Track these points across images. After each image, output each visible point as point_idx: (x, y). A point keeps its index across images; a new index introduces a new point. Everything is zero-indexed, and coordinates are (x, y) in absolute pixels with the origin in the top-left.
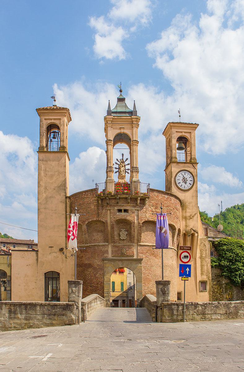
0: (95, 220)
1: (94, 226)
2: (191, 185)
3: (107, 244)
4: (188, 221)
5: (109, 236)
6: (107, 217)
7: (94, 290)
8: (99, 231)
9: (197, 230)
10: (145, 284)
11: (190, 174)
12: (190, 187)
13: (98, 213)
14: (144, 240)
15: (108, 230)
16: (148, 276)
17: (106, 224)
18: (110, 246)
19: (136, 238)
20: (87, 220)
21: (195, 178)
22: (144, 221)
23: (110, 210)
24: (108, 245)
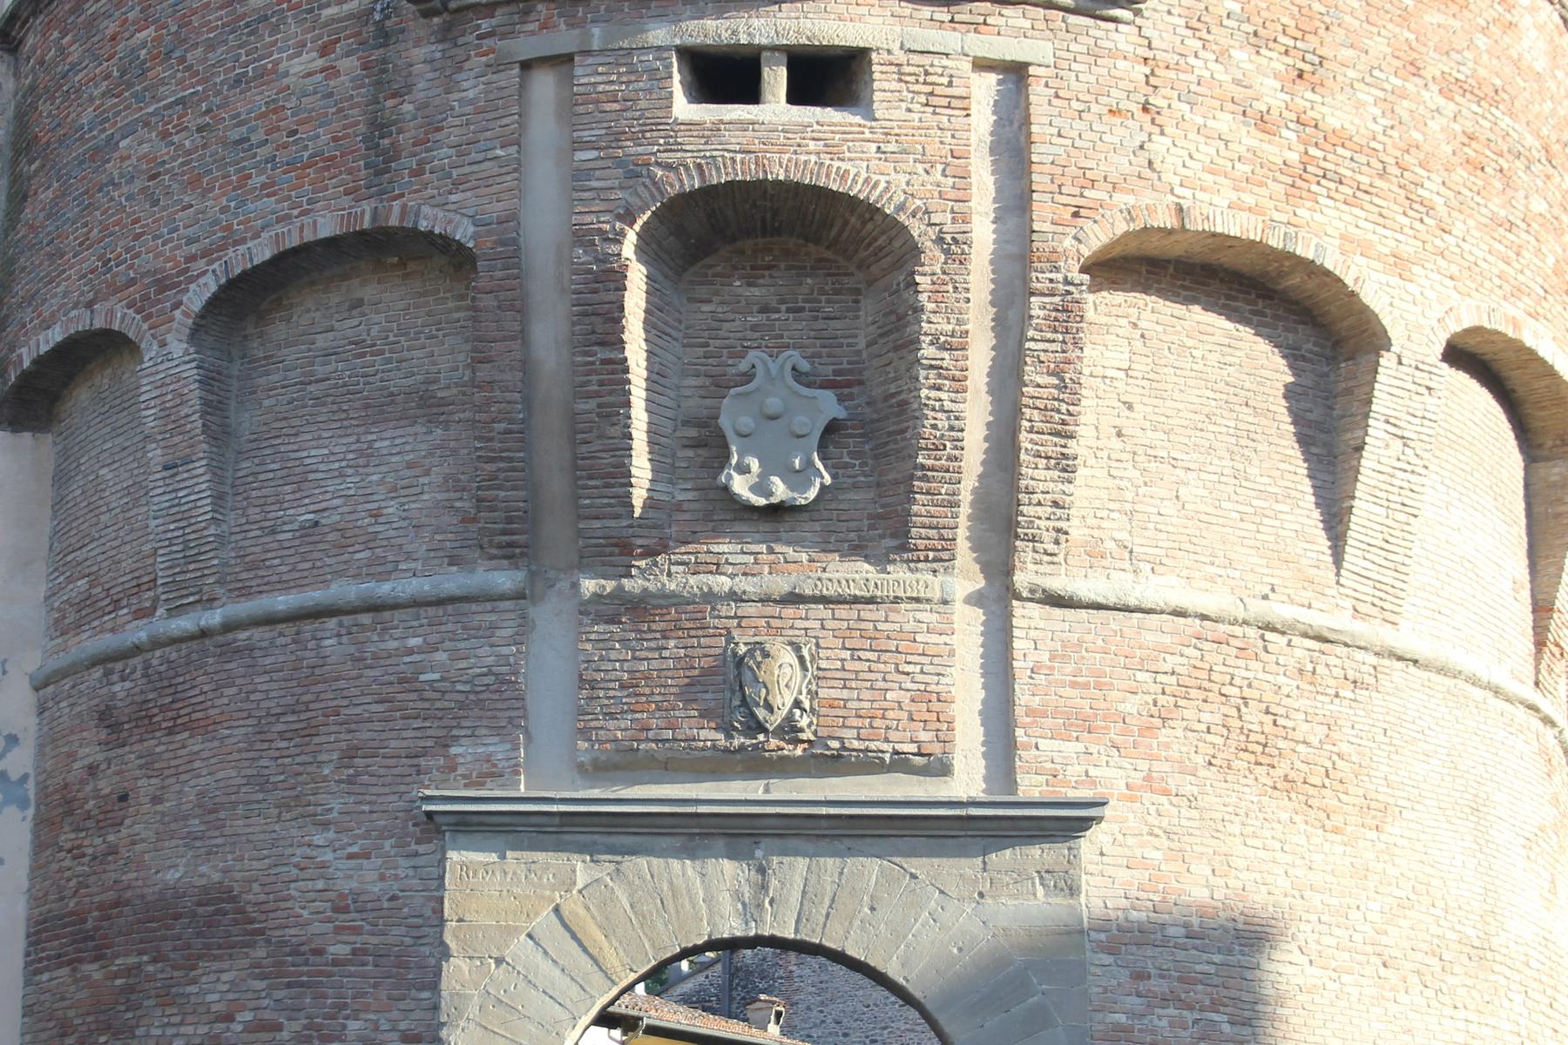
0: (327, 226)
1: (321, 341)
3: (505, 579)
5: (551, 455)
6: (518, 166)
8: (379, 410)
14: (1117, 528)
15: (526, 366)
17: (486, 274)
18: (551, 621)
20: (206, 253)
22: (1121, 228)
23: (564, 60)
24: (520, 596)
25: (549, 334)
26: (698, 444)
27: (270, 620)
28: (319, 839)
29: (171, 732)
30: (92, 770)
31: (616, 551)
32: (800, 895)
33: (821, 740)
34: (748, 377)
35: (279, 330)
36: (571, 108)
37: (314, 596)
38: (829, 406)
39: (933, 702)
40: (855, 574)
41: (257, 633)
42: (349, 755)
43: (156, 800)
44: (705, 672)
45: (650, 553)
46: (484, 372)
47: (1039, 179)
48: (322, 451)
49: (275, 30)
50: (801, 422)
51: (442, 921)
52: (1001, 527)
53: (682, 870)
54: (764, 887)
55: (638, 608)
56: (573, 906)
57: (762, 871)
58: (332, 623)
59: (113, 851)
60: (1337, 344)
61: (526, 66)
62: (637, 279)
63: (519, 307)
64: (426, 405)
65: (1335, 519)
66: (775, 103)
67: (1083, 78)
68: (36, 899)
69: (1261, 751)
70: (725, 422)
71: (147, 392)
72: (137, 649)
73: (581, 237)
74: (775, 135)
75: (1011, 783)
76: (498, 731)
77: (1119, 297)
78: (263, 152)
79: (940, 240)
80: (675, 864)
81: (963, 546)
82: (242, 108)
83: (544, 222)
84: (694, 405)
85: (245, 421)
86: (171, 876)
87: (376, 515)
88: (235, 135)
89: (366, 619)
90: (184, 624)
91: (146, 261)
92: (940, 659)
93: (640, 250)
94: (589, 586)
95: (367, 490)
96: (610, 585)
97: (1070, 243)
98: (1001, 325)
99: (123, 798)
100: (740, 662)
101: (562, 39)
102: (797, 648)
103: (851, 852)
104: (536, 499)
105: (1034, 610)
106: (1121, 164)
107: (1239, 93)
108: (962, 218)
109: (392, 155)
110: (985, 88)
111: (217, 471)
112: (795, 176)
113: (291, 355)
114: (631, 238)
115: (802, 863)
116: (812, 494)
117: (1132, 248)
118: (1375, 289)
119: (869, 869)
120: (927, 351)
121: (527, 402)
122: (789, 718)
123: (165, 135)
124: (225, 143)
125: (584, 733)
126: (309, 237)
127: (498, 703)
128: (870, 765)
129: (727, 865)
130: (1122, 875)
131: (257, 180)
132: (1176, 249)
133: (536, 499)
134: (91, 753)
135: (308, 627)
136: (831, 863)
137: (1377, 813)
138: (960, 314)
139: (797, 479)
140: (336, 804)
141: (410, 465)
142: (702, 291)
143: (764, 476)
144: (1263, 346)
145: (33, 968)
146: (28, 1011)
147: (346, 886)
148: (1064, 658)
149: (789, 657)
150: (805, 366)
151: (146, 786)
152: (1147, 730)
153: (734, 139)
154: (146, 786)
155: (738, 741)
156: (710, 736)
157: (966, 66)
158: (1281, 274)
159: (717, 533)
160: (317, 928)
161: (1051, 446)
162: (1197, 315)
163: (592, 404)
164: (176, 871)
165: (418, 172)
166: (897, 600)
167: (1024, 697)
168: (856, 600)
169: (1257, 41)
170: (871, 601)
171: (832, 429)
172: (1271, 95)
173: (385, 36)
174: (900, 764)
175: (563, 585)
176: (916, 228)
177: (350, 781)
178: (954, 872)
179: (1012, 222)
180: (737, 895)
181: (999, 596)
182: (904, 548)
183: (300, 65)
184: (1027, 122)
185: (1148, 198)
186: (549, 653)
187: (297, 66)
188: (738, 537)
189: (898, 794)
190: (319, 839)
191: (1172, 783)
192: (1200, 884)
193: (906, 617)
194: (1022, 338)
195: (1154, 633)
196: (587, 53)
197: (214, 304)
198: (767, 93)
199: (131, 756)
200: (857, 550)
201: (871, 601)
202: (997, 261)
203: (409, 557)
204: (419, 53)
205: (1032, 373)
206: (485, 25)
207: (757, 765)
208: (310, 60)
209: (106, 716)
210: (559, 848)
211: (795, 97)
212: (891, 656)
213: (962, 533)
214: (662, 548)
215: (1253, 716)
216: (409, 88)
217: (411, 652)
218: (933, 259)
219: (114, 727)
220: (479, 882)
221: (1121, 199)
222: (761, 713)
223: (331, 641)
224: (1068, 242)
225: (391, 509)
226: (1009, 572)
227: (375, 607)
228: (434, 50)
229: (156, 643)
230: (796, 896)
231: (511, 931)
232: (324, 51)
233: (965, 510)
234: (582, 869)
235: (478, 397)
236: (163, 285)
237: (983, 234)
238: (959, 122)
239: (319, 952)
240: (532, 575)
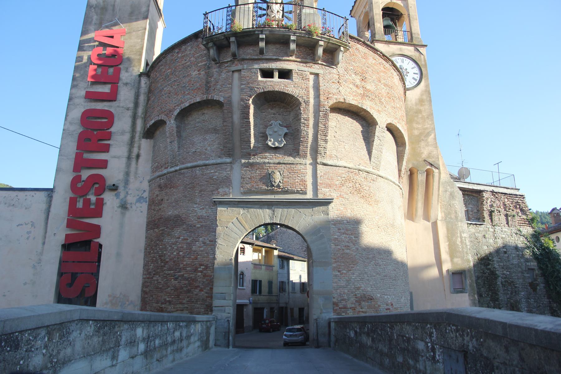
0: (198, 100)
1: (197, 120)
2: (416, 80)
3: (228, 160)
5: (237, 139)
6: (231, 88)
7: (185, 289)
10: (339, 271)
11: (412, 63)
12: (415, 84)
14: (334, 153)
15: (232, 123)
16: (348, 247)
18: (236, 167)
20: (178, 105)
21: (423, 69)
22: (335, 101)
23: (239, 71)
24: (231, 163)
25: (236, 117)
26: (262, 137)
27: (187, 168)
28: (195, 206)
29: (170, 188)
30: (157, 195)
31: (248, 155)
32: (280, 215)
33: (284, 188)
34: (271, 125)
35: (190, 119)
36: (240, 79)
37: (195, 164)
38: (285, 130)
39: (304, 182)
40: (290, 159)
41: (185, 170)
42: (201, 191)
43: (167, 200)
44: (264, 176)
45: (254, 155)
46: (225, 124)
47: (321, 92)
48: (197, 139)
49: (190, 68)
50: (280, 133)
51: (217, 220)
52: (315, 151)
53: (260, 211)
54: (274, 214)
55: (252, 165)
56: (240, 218)
57: (274, 211)
58: (198, 168)
59: (160, 209)
60: (369, 124)
61: (233, 72)
62: (252, 107)
63: (231, 112)
65: (370, 153)
66: (276, 78)
67: (328, 77)
68: (148, 218)
69: (359, 191)
70: (267, 133)
71: (167, 129)
72: (165, 174)
73: (242, 100)
74: (276, 84)
75: (317, 196)
76: (227, 187)
77: (334, 114)
78: (188, 88)
79: (304, 102)
80: (258, 210)
81: (308, 155)
82: (184, 81)
83: (236, 97)
84: (262, 130)
85: (184, 134)
86: (170, 213)
87: (206, 149)
88: (183, 85)
89: (204, 167)
90: (173, 169)
91: (168, 107)
92: (305, 174)
93: (253, 102)
94: (243, 161)
95: (204, 144)
96: (247, 161)
97: (327, 104)
98: (315, 116)
99: (162, 200)
100: (270, 174)
101: (239, 67)
102: (280, 172)
103: (289, 208)
104: (234, 146)
105: (321, 166)
106: (335, 91)
107: (353, 81)
108: (308, 98)
109: (210, 87)
110: (312, 77)
111: (179, 143)
112: (279, 90)
113: (192, 123)
114: (251, 100)
115: (281, 210)
116: (282, 145)
117: (336, 106)
118: (375, 115)
119: (292, 211)
120: (302, 121)
121: (232, 129)
122: (278, 184)
123: (172, 86)
124: (181, 87)
125: (242, 187)
126: (195, 101)
127: (227, 182)
128: (293, 192)
129: (267, 210)
130: (336, 212)
131: (187, 93)
132: (343, 106)
133: (234, 146)
134: (157, 193)
135: (194, 169)
136: (286, 210)
137: (377, 202)
138: (308, 114)
139: (280, 142)
140: (198, 200)
141: (212, 141)
142: (264, 111)
143: (274, 142)
144: (357, 124)
145: (147, 230)
146: (146, 238)
147: (200, 214)
148: (326, 174)
149: (278, 173)
150: (281, 123)
151: (166, 198)
152: (340, 187)
153: (269, 84)
154: (166, 198)
155: (269, 188)
156: (264, 187)
157: (309, 73)
158: (360, 112)
159: (266, 152)
160: (195, 222)
161: (324, 138)
162: (347, 118)
163: (244, 129)
164: (171, 212)
165: (214, 90)
166: (297, 164)
167: (319, 181)
168: (290, 164)
169: (356, 74)
170: (293, 164)
171: (286, 134)
172: (358, 82)
173: (209, 68)
174: (298, 192)
175: (239, 161)
176: (300, 99)
177: (201, 196)
178: (308, 211)
179: (317, 99)
180: (269, 216)
181: (315, 164)
182: (298, 155)
183: (194, 73)
184: (319, 83)
185: (339, 97)
186: (236, 173)
187: (194, 74)
188: (269, 153)
189: (297, 198)
190: (195, 206)
191: (344, 196)
192: (349, 213)
193: (299, 167)
194: (319, 119)
195: (341, 170)
196: (243, 69)
197: (179, 114)
198: (275, 77)
199: (163, 192)
200: (290, 155)
201: (293, 164)
202: (314, 106)
203: (212, 157)
204: (215, 70)
205: (320, 125)
206: (226, 65)
207: (273, 192)
208: (196, 72)
209: (160, 186)
210: (237, 207)
211: (279, 78)
212: (296, 174)
213: (308, 152)
214: (257, 155)
215: (357, 185)
216: (213, 76)
217: (212, 173)
218: (303, 105)
219: (161, 188)
220: (223, 213)
221: (335, 97)
222: (273, 183)
223: (198, 171)
224: (326, 103)
225: (209, 148)
226: (316, 159)
227: (206, 165)
228: (217, 70)
229: (168, 173)
230: (280, 215)
231: (229, 222)
232: (199, 71)
233: (309, 148)
234: (242, 211)
235: (224, 128)
236: (170, 111)
237: (312, 101)
238: (308, 82)
239: (195, 226)
240: (233, 159)
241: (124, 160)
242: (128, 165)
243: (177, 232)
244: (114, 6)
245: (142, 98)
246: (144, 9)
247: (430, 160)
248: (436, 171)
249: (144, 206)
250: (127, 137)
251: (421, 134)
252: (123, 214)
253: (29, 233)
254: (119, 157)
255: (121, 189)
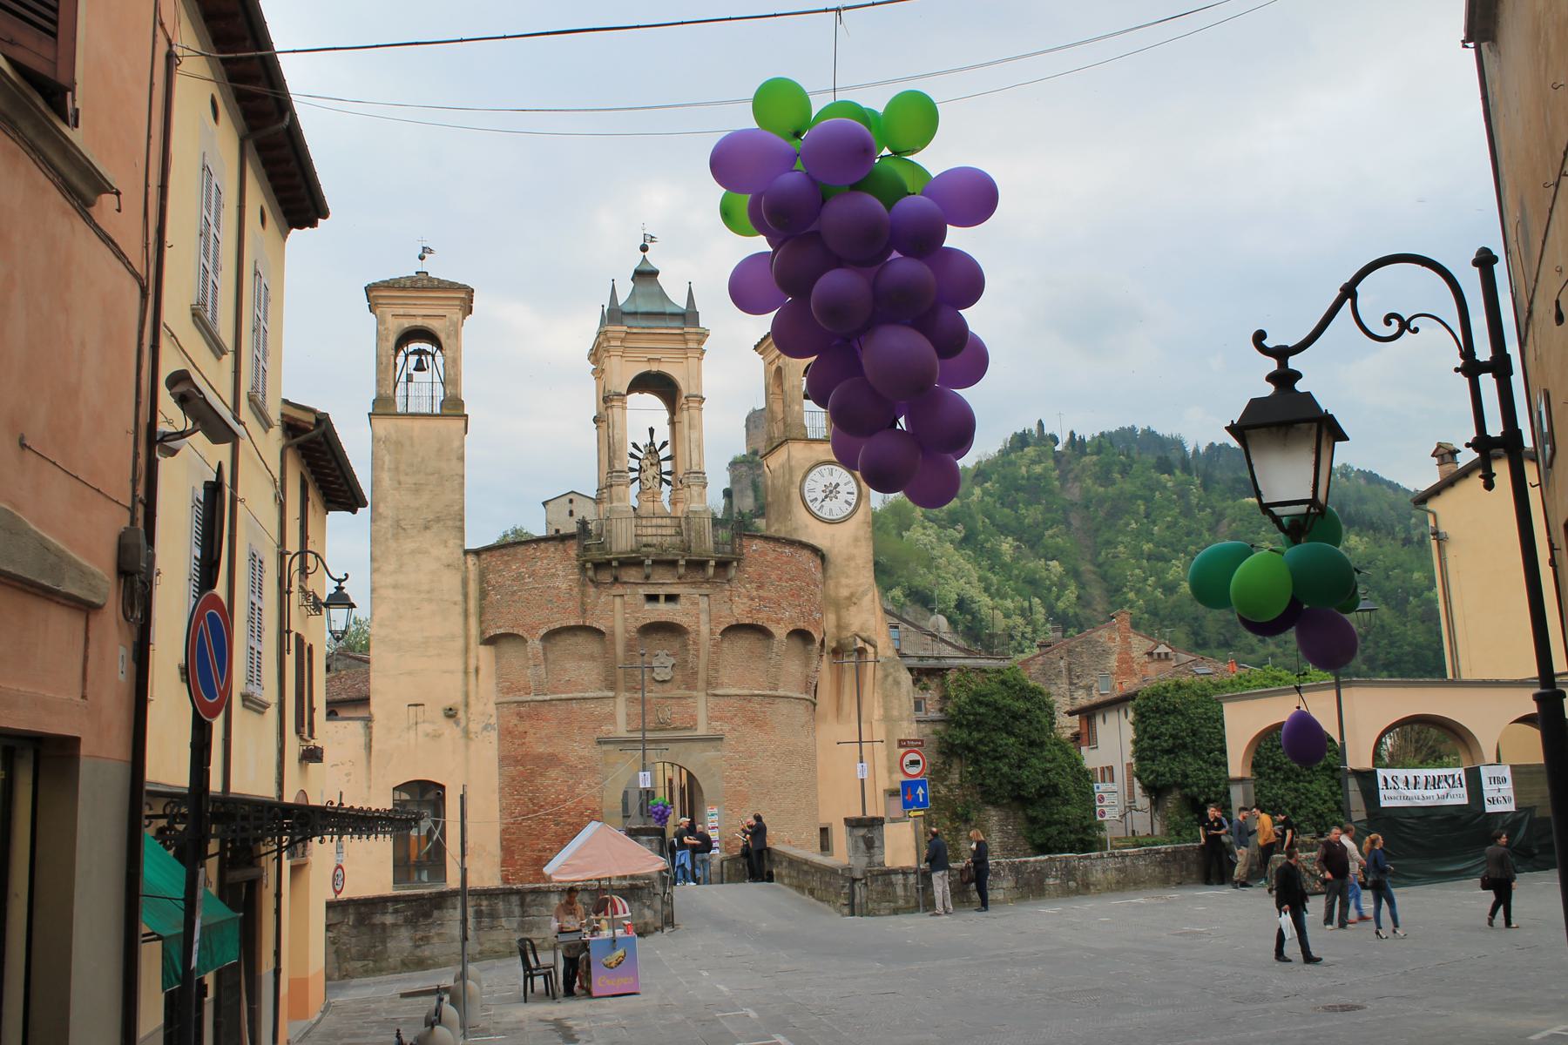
3: (611, 694)
4: (844, 613)
9: (874, 637)
13: (583, 604)
16: (740, 784)
19: (702, 675)
38: (673, 661)
63: (613, 643)
64: (592, 658)
69: (752, 721)
145: (501, 767)
199: (527, 724)
204: (592, 590)
241: (460, 676)
242: (466, 684)
243: (553, 773)
244: (411, 438)
245: (473, 588)
246: (456, 444)
247: (864, 635)
248: (870, 649)
249: (494, 736)
250: (460, 643)
251: (852, 595)
252: (467, 747)
253: (348, 775)
254: (452, 672)
255: (461, 714)
